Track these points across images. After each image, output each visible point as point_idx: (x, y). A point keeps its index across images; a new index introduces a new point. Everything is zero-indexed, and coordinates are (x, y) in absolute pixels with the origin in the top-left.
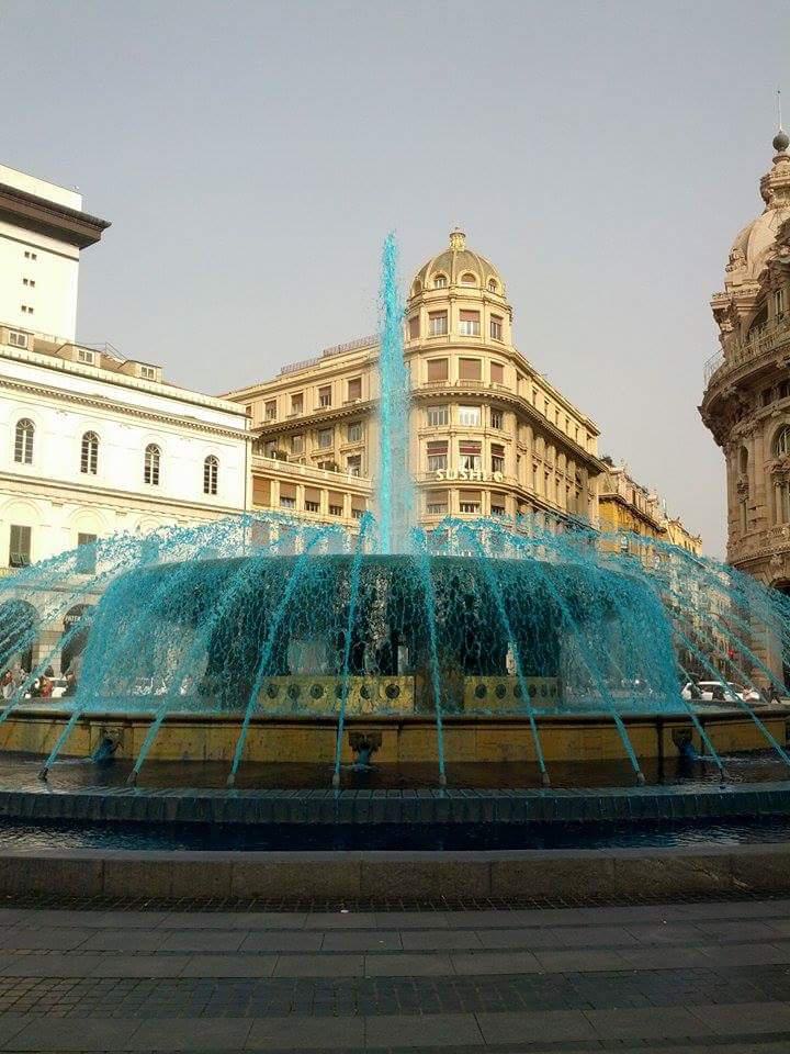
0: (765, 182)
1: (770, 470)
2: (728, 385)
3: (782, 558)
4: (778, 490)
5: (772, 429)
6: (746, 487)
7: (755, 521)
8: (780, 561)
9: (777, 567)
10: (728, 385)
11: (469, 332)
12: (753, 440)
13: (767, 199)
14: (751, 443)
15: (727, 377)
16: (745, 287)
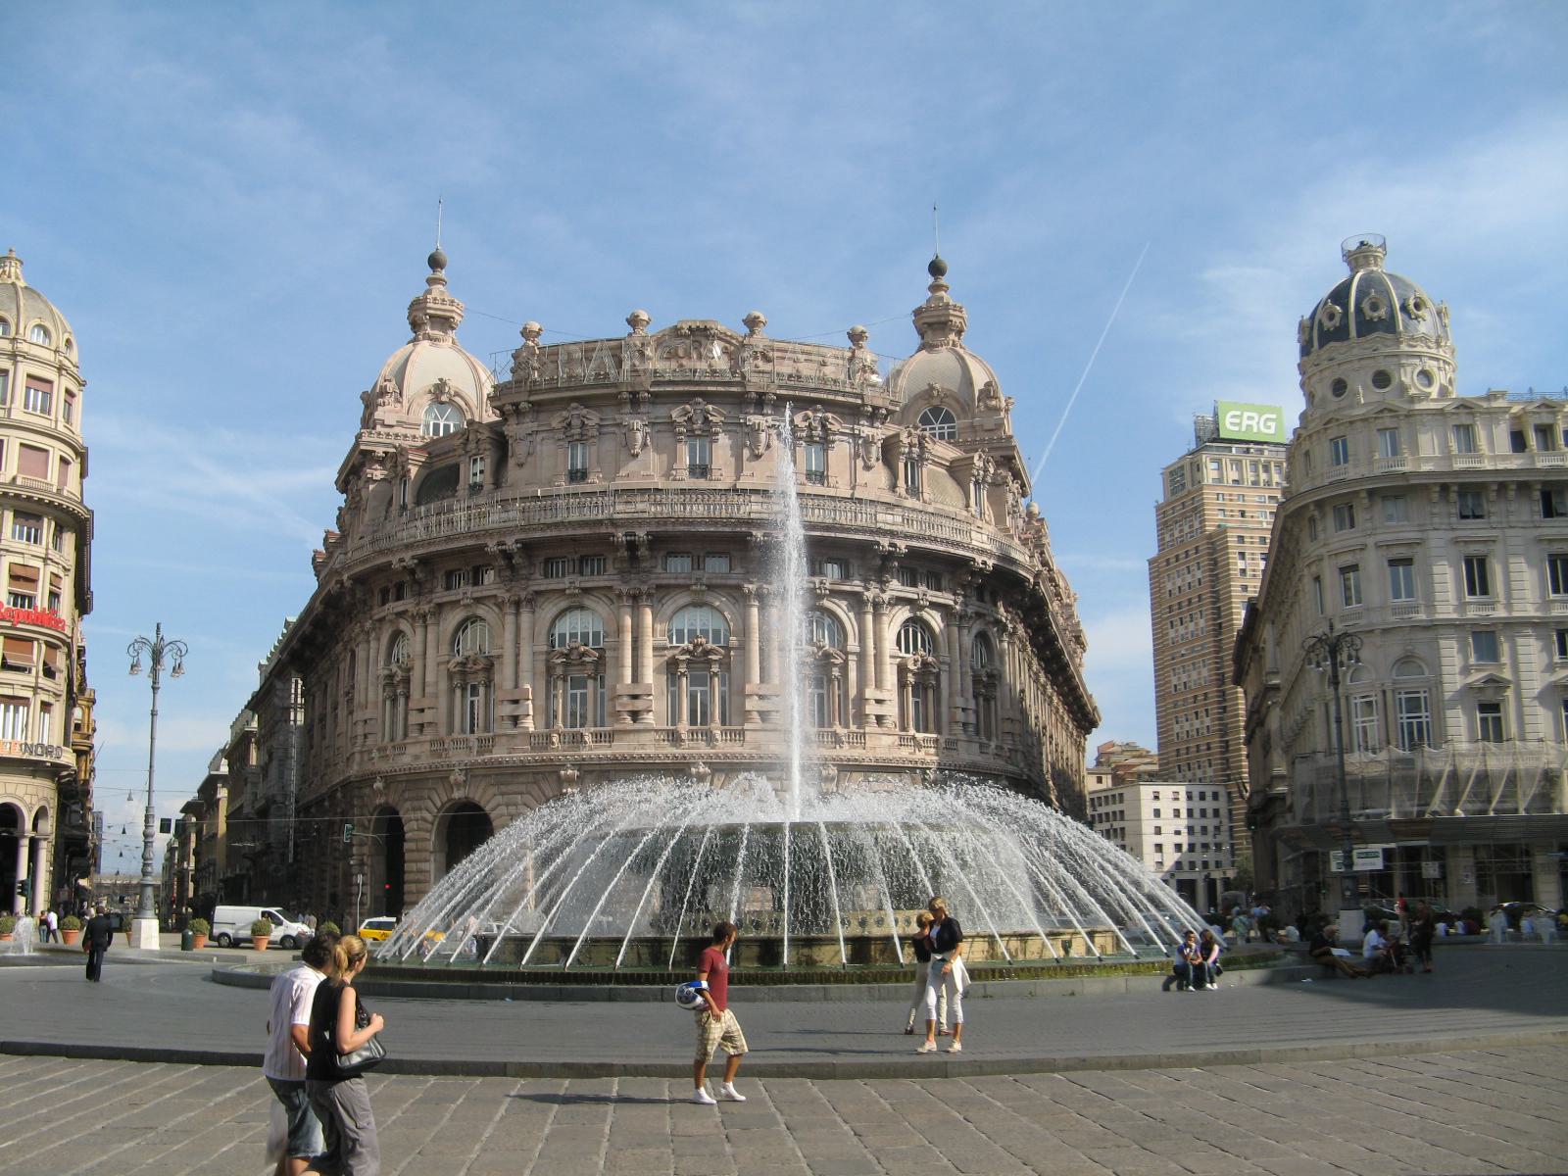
0: (417, 305)
1: (451, 665)
2: (407, 556)
3: (466, 775)
4: (458, 692)
5: (453, 618)
6: (407, 681)
7: (422, 726)
8: (462, 778)
9: (458, 785)
10: (407, 556)
11: (35, 409)
12: (426, 627)
13: (416, 325)
14: (420, 631)
15: (408, 547)
16: (397, 430)
